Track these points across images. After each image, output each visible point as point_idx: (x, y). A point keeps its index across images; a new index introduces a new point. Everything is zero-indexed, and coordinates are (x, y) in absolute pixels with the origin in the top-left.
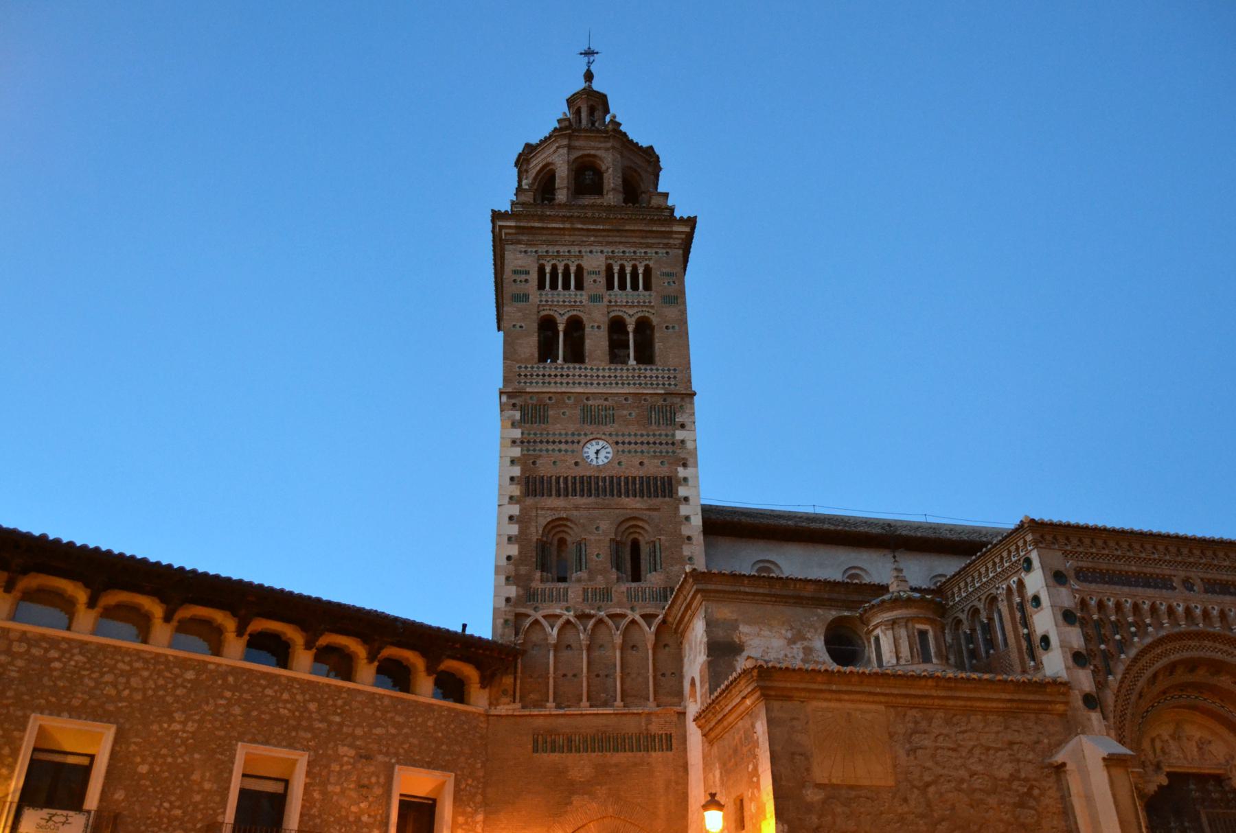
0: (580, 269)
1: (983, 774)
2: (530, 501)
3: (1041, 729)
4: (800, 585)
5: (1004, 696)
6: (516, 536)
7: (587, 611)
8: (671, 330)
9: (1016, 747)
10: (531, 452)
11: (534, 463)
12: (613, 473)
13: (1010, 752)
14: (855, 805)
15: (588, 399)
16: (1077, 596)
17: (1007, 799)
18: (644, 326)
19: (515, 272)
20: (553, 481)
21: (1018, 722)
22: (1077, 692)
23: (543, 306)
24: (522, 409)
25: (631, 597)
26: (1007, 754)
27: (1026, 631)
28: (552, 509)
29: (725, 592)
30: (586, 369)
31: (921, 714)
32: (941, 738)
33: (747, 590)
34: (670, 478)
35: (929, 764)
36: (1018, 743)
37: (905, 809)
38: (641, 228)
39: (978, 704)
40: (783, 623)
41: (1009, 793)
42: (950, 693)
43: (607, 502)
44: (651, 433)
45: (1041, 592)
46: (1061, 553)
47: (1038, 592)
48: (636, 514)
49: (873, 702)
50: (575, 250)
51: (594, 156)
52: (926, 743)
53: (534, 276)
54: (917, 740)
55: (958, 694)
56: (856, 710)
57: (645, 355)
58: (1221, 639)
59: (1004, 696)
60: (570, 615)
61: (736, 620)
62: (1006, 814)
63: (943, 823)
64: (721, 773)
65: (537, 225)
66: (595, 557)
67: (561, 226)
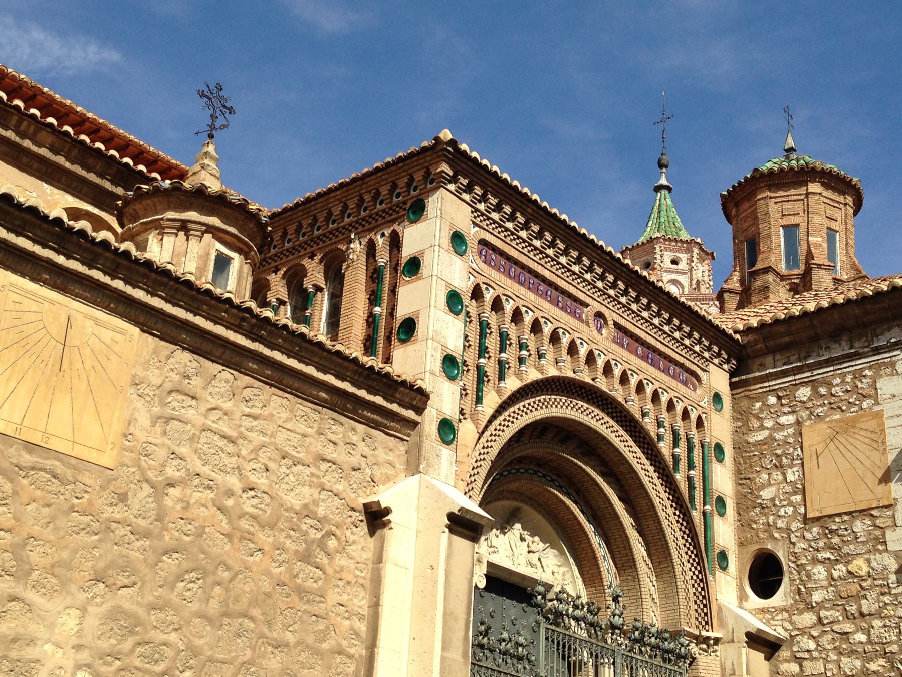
3: (367, 451)
4: (29, 126)
9: (324, 466)
13: (313, 470)
14: (25, 482)
17: (288, 542)
21: (340, 429)
22: (434, 412)
27: (377, 310)
31: (195, 364)
32: (215, 415)
35: (183, 450)
36: (329, 462)
37: (118, 513)
41: (292, 533)
45: (426, 255)
46: (470, 209)
47: (422, 253)
52: (190, 414)
54: (175, 404)
56: (86, 316)
62: (279, 566)
63: (176, 555)
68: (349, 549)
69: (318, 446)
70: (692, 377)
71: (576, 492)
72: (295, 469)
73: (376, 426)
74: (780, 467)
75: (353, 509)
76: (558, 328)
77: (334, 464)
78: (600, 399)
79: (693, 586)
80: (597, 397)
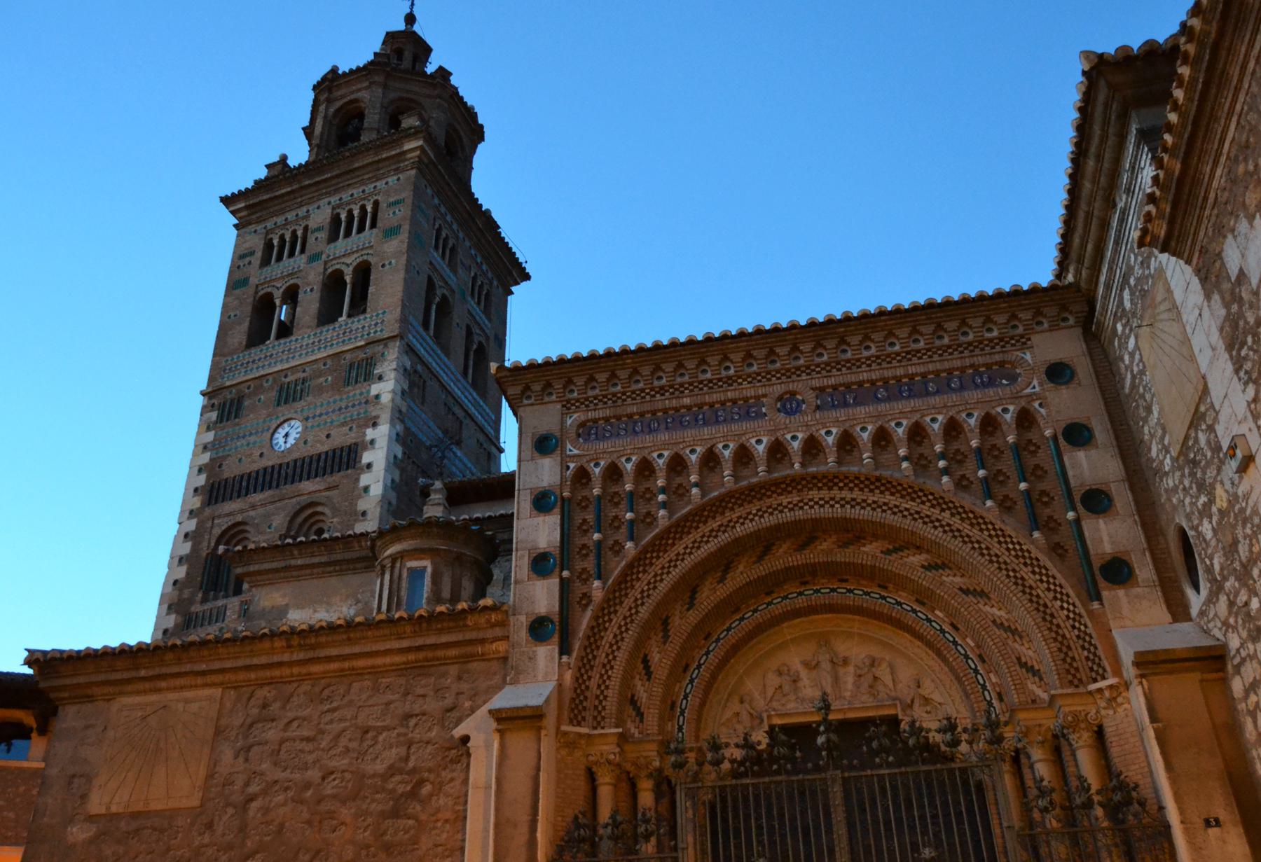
1: (343, 771)
2: (208, 511)
5: (396, 645)
6: (187, 556)
8: (387, 267)
11: (220, 466)
15: (286, 376)
16: (572, 465)
22: (523, 618)
26: (394, 735)
29: (277, 570)
33: (300, 562)
34: (356, 444)
36: (417, 715)
38: (370, 160)
39: (361, 663)
40: (347, 597)
42: (310, 654)
43: (284, 491)
44: (344, 397)
48: (315, 498)
49: (206, 685)
50: (302, 212)
51: (356, 101)
53: (259, 254)
55: (323, 653)
56: (178, 701)
57: (360, 304)
58: (841, 481)
59: (396, 645)
61: (287, 605)
65: (266, 197)
67: (289, 189)
68: (447, 788)
69: (407, 708)
70: (1002, 373)
71: (880, 586)
72: (381, 738)
73: (469, 658)
74: (1149, 409)
75: (450, 749)
76: (714, 445)
77: (424, 714)
78: (815, 481)
79: (1074, 627)
80: (808, 482)
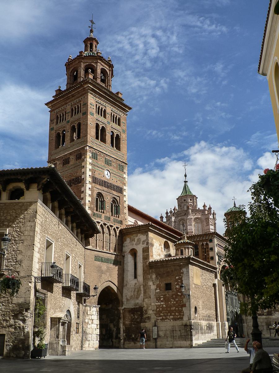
0: (105, 111)
2: (94, 184)
7: (105, 223)
10: (94, 169)
11: (94, 172)
12: (110, 182)
18: (118, 137)
19: (91, 104)
20: (98, 180)
23: (97, 119)
24: (92, 153)
25: (115, 221)
28: (98, 189)
30: (106, 146)
60: (102, 223)
64: (156, 276)
66: (107, 207)
